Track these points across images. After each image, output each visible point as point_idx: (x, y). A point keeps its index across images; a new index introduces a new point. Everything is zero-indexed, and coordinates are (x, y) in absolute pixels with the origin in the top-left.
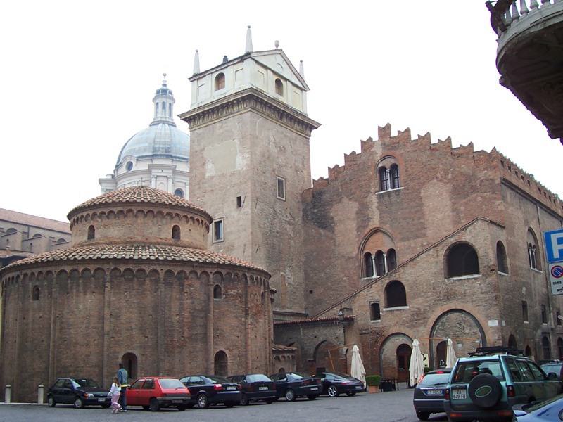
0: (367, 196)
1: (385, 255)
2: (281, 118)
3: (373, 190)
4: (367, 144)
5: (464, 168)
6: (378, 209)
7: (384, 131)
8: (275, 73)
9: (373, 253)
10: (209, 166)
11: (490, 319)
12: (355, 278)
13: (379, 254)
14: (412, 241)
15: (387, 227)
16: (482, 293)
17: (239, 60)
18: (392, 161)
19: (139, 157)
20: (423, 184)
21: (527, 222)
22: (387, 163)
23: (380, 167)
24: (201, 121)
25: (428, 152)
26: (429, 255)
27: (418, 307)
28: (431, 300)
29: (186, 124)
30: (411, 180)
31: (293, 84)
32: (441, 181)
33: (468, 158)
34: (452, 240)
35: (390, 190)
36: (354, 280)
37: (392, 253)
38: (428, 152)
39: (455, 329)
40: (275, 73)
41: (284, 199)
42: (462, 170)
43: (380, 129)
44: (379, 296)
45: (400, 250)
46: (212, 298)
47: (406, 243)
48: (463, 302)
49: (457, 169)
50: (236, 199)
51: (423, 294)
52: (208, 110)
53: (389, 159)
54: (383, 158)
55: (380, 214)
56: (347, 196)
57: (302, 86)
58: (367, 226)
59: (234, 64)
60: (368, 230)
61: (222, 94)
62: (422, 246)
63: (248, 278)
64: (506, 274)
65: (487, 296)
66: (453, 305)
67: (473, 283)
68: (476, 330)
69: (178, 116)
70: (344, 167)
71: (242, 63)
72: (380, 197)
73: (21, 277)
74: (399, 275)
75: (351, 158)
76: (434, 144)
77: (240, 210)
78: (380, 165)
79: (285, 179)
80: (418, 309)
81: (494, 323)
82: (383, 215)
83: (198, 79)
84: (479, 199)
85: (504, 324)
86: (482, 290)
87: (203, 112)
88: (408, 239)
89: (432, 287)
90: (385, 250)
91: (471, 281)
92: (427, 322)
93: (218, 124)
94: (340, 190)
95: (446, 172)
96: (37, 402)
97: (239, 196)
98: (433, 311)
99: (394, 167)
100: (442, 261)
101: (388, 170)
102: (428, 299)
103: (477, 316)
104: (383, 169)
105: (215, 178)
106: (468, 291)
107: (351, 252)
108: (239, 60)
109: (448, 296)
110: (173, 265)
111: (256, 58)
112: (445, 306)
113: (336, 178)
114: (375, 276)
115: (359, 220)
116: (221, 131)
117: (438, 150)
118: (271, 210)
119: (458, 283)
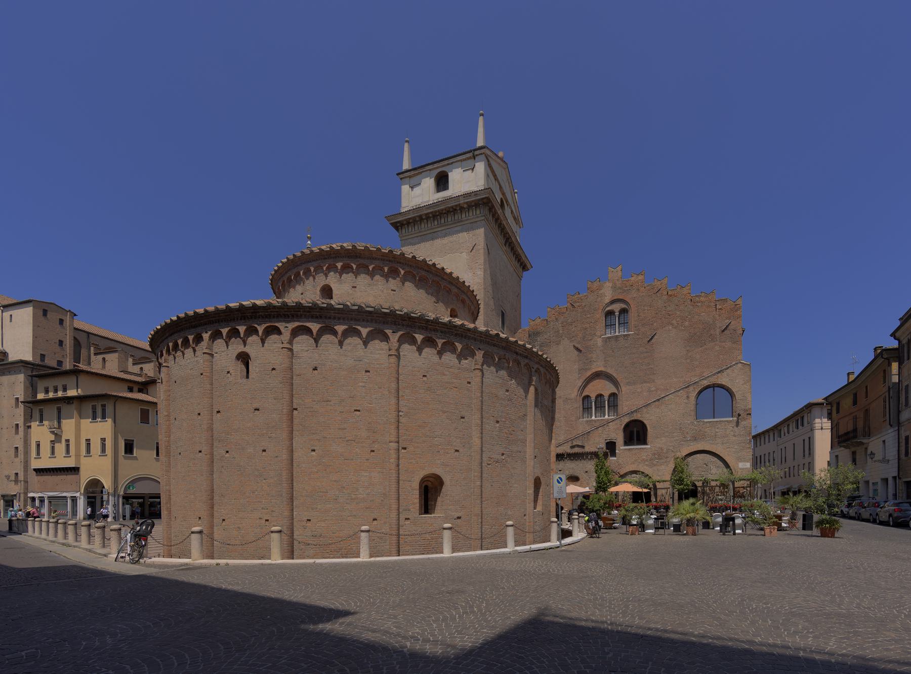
6: (604, 353)
13: (600, 396)
15: (610, 371)
18: (623, 306)
23: (608, 311)
33: (709, 306)
35: (617, 334)
37: (613, 395)
38: (665, 297)
52: (426, 214)
54: (613, 302)
60: (589, 373)
61: (444, 197)
71: (473, 160)
94: (561, 332)
99: (624, 311)
104: (610, 313)
108: (468, 155)
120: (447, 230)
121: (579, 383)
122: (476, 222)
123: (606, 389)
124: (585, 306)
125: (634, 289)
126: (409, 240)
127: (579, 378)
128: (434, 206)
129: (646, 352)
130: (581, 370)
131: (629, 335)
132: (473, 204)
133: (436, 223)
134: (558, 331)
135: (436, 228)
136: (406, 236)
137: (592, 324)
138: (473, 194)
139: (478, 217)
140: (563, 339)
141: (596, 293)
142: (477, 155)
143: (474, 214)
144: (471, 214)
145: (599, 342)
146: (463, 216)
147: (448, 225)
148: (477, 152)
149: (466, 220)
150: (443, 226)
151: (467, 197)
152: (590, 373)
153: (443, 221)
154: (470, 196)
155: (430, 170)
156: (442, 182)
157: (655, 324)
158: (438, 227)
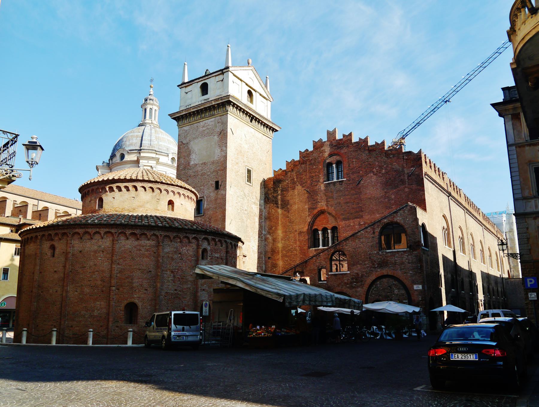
0: (317, 185)
1: (329, 231)
2: (251, 121)
3: (321, 180)
4: (318, 145)
5: (396, 166)
7: (331, 134)
8: (247, 84)
9: (320, 228)
10: (193, 156)
11: (415, 284)
12: (306, 248)
14: (351, 221)
16: (409, 263)
17: (219, 73)
18: (338, 158)
19: (130, 150)
20: (362, 176)
21: (442, 209)
22: (334, 159)
24: (188, 120)
25: (367, 152)
26: (367, 232)
27: (356, 271)
28: (368, 267)
29: (175, 122)
30: (353, 173)
31: (260, 95)
32: (375, 175)
33: (398, 158)
34: (385, 220)
35: (335, 180)
36: (304, 250)
37: (334, 229)
39: (386, 290)
40: (247, 84)
41: (251, 185)
42: (394, 167)
43: (328, 132)
44: (325, 262)
45: (342, 228)
46: (200, 258)
47: (347, 222)
48: (393, 270)
49: (390, 166)
50: (214, 183)
51: (361, 262)
52: (193, 112)
53: (335, 157)
55: (327, 199)
56: (301, 185)
57: (268, 98)
58: (316, 208)
59: (216, 76)
60: (316, 211)
61: (205, 100)
62: (360, 224)
63: (229, 244)
64: (427, 249)
65: (414, 265)
66: (385, 271)
67: (402, 255)
68: (403, 292)
69: (169, 115)
70: (299, 161)
72: (327, 186)
73: (39, 237)
74: (342, 246)
75: (304, 155)
76: (371, 146)
77: (218, 192)
78: (328, 161)
79: (252, 168)
80: (357, 273)
81: (418, 287)
82: (328, 200)
83: (186, 87)
84: (407, 190)
85: (426, 289)
86: (409, 260)
87: (190, 113)
88: (348, 219)
89: (368, 257)
90: (329, 226)
91: (400, 253)
92: (364, 285)
93: (201, 123)
94: (295, 180)
95: (381, 167)
96: (87, 344)
97: (217, 180)
98: (369, 276)
100: (378, 237)
101: (334, 165)
102: (365, 266)
103: (405, 281)
104: (330, 165)
105: (198, 166)
106: (397, 261)
107: (303, 228)
108: (219, 73)
109: (383, 264)
110: (171, 231)
111: (232, 71)
112: (379, 273)
113: (292, 170)
114: (321, 247)
115: (310, 203)
116: (204, 129)
117: (375, 151)
118: (242, 193)
119: (389, 254)
120: (206, 121)
121: (309, 219)
122: (223, 115)
123: (331, 223)
124: (312, 159)
125: (345, 146)
126: (183, 128)
127: (309, 216)
128: (197, 107)
129: (356, 194)
130: (311, 209)
131: (343, 181)
132: (221, 104)
133: (199, 117)
134: (293, 179)
135: (199, 120)
136: (181, 125)
137: (317, 173)
138: (220, 99)
139: (224, 112)
140: (297, 185)
141: (318, 150)
142: (225, 72)
143: (222, 110)
144: (220, 110)
145: (322, 187)
146: (215, 112)
147: (206, 118)
148: (224, 71)
149: (217, 114)
150: (203, 118)
151: (216, 101)
152: (317, 211)
153: (203, 115)
154: (218, 100)
155: (197, 82)
156: (204, 89)
157: (361, 172)
158: (200, 119)
